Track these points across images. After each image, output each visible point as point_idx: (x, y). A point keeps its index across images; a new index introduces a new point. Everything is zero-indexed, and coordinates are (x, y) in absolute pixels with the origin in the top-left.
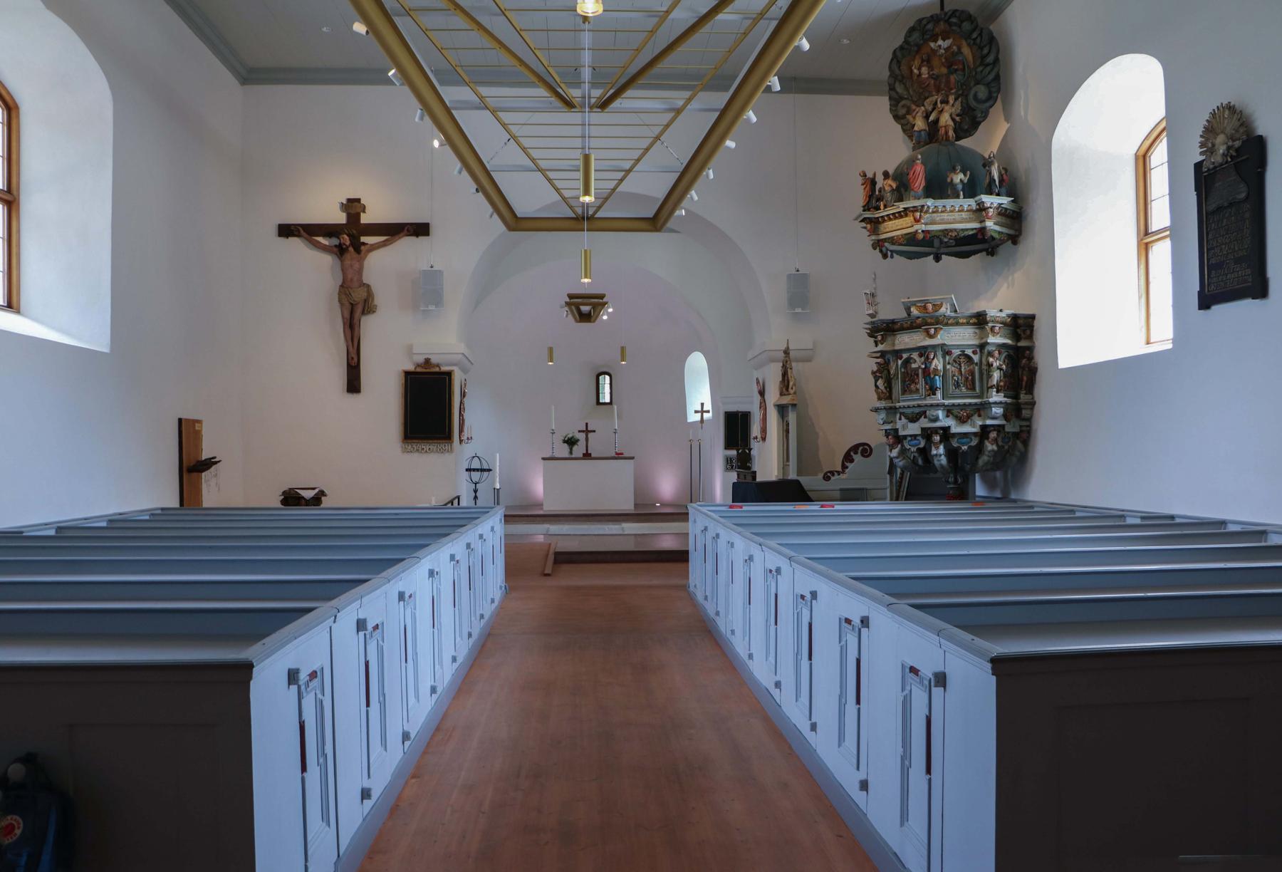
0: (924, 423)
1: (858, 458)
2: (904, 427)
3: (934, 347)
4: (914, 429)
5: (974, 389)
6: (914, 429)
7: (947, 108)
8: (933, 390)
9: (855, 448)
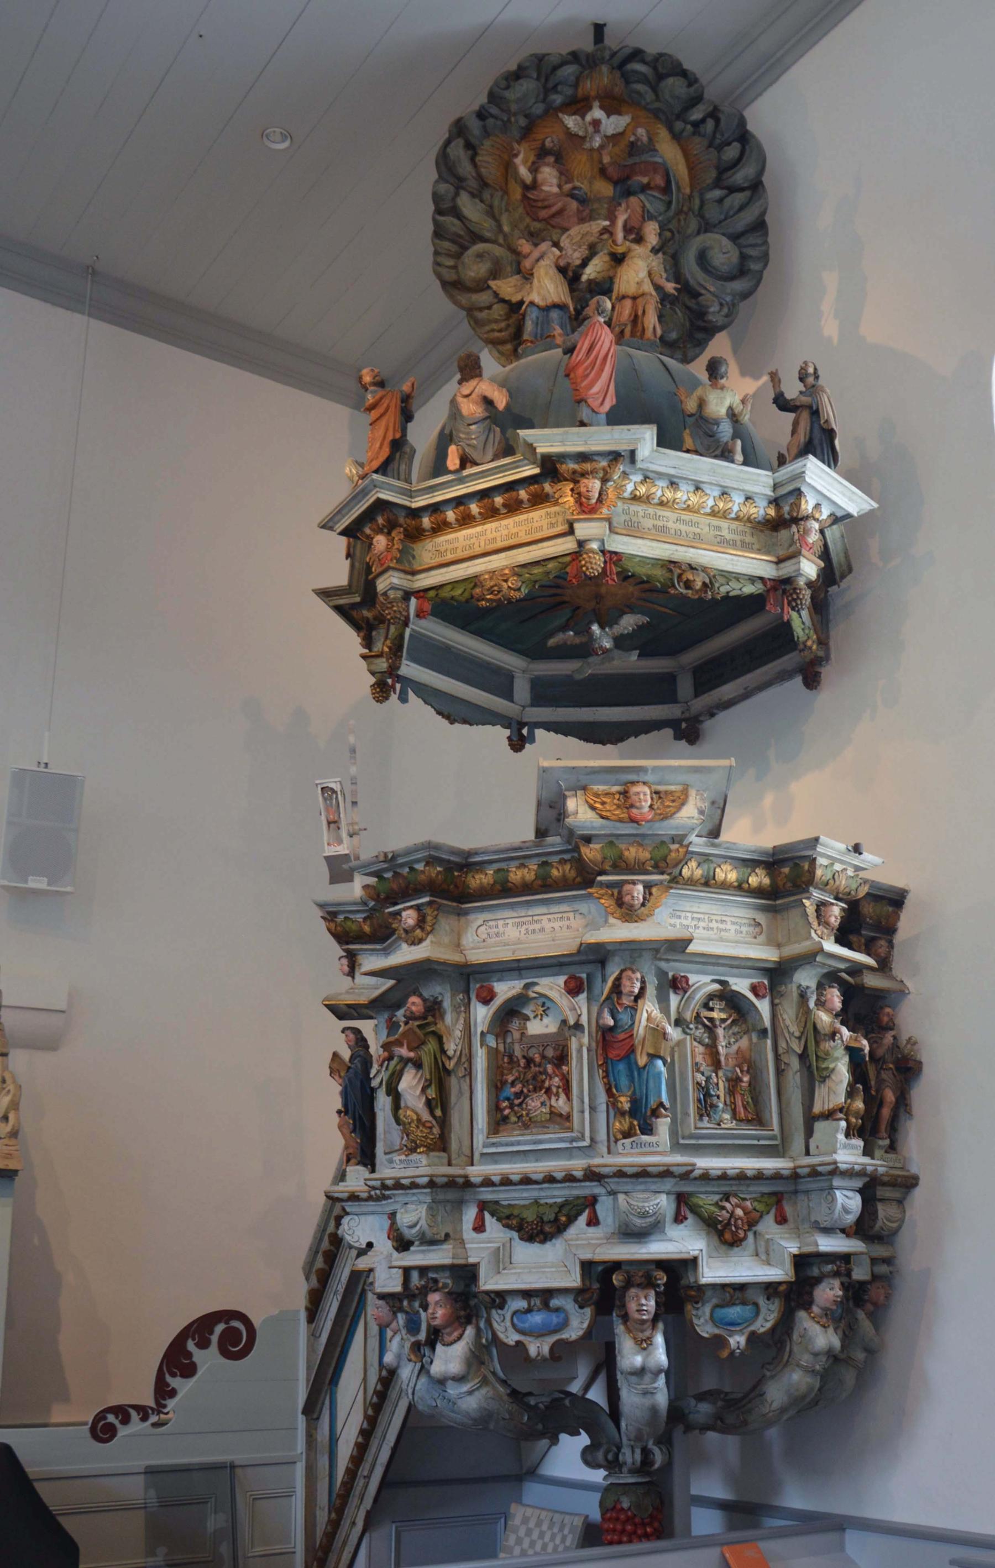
1: (207, 1359)
2: (501, 1260)
4: (548, 1265)
5: (758, 1120)
6: (548, 1265)
7: (638, 250)
8: (641, 1117)
9: (200, 1329)
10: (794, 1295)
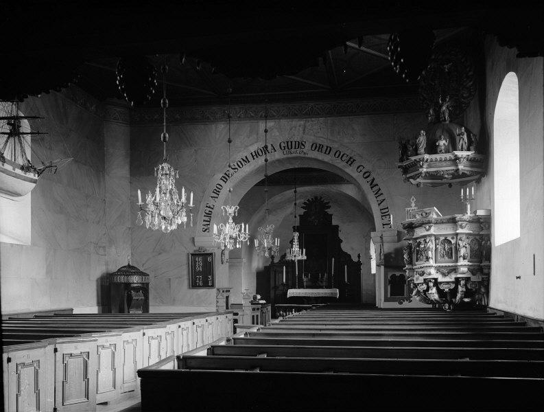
0: (426, 277)
2: (417, 279)
3: (430, 236)
6: (421, 279)
8: (428, 259)
10: (457, 281)
